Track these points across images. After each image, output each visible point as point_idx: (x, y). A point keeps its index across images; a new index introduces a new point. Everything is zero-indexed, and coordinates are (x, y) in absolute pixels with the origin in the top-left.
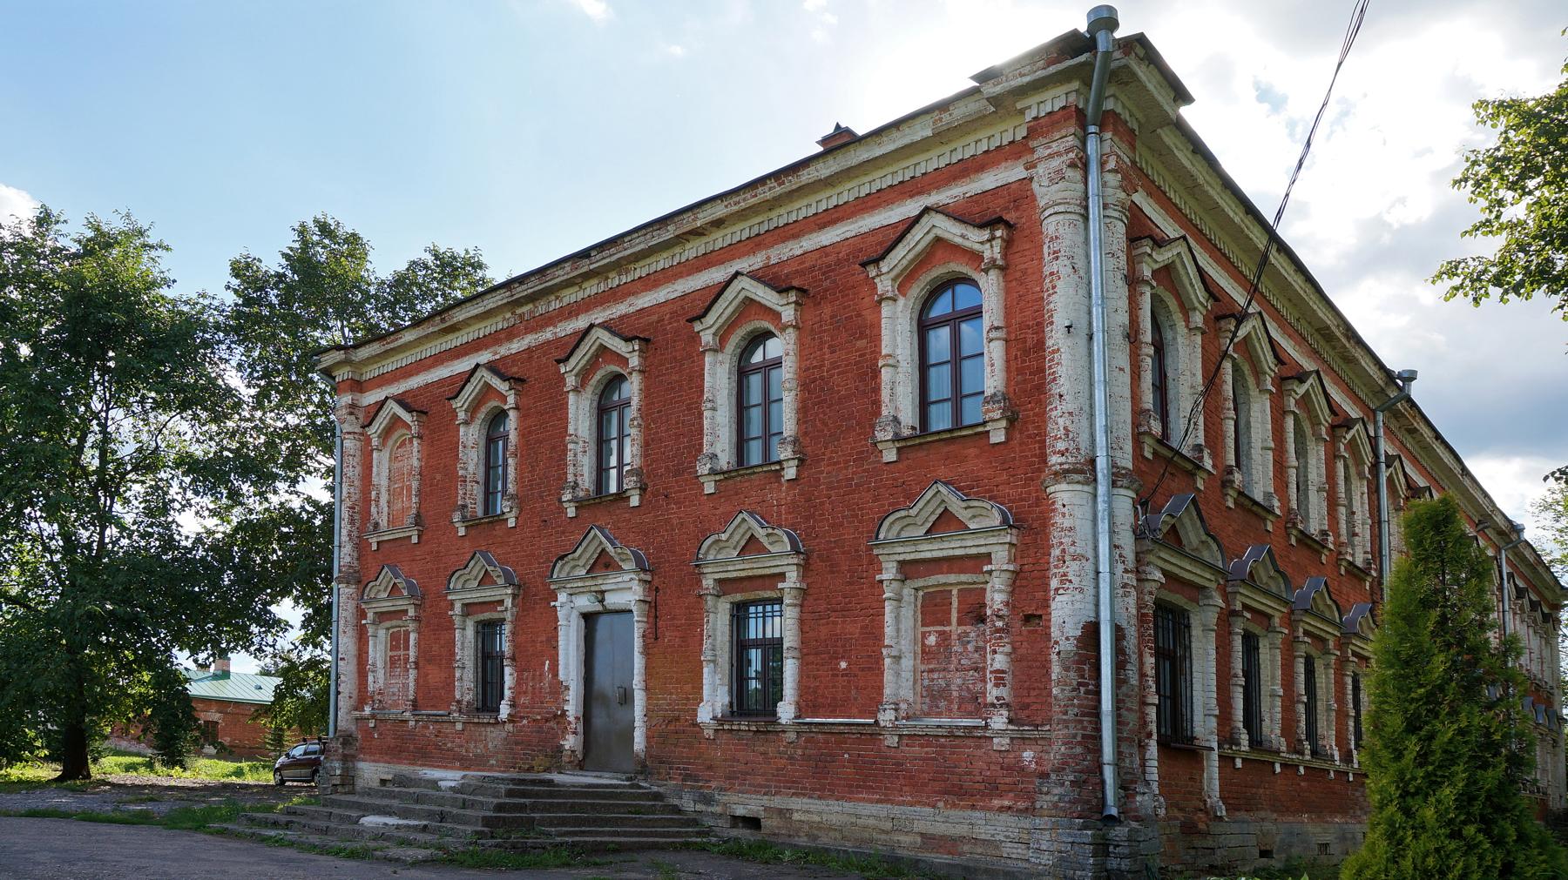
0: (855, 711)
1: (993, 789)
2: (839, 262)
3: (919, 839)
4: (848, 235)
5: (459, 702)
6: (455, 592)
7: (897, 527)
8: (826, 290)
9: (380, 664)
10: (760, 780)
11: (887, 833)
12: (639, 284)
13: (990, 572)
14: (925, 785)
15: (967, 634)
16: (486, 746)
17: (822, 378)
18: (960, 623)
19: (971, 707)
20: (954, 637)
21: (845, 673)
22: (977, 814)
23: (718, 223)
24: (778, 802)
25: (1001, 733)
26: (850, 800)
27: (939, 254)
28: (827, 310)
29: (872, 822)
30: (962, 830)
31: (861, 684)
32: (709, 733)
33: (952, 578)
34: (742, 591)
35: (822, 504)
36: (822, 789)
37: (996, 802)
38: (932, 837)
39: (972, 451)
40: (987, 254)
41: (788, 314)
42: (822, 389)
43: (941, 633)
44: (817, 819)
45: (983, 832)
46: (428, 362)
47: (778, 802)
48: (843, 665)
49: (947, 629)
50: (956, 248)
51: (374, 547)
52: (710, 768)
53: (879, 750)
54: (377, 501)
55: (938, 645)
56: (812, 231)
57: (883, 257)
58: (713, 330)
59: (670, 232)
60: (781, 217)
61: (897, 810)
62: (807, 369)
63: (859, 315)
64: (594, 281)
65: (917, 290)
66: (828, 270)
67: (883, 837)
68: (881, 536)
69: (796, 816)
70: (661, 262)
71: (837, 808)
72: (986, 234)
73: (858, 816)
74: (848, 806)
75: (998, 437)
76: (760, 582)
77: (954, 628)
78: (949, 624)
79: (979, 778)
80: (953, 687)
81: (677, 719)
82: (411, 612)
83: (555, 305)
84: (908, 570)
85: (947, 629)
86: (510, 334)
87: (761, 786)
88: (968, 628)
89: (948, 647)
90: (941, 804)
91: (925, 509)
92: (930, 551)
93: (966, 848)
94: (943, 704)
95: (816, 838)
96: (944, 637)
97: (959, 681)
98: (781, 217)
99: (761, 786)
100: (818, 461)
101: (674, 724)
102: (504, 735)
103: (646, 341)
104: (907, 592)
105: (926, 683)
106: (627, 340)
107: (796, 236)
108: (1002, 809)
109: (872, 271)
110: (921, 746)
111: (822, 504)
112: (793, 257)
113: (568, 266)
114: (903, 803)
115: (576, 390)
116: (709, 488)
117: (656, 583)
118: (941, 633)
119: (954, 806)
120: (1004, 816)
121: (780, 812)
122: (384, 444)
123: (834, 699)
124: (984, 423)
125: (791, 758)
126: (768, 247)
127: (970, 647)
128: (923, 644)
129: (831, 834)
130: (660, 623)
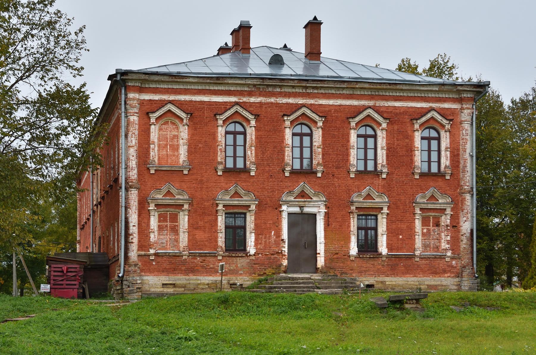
0: (405, 251)
1: (445, 271)
2: (400, 113)
8: (396, 121)
10: (372, 273)
15: (435, 229)
17: (394, 148)
18: (433, 226)
19: (436, 250)
21: (401, 239)
24: (380, 279)
25: (448, 257)
26: (405, 277)
28: (396, 127)
29: (412, 283)
30: (439, 283)
31: (407, 243)
33: (430, 214)
34: (364, 211)
36: (394, 274)
37: (446, 275)
38: (430, 286)
39: (440, 180)
41: (384, 125)
43: (428, 229)
45: (444, 283)
47: (380, 279)
48: (401, 237)
55: (427, 232)
56: (392, 100)
61: (420, 279)
62: (389, 144)
63: (406, 132)
66: (396, 114)
69: (387, 283)
75: (448, 177)
76: (371, 209)
77: (431, 228)
78: (430, 226)
81: (337, 254)
89: (430, 233)
94: (428, 249)
96: (429, 230)
100: (393, 174)
109: (415, 122)
112: (384, 106)
114: (420, 277)
119: (435, 277)
120: (450, 278)
121: (382, 282)
123: (398, 247)
125: (383, 265)
126: (376, 100)
127: (436, 233)
129: (399, 287)
130: (330, 220)
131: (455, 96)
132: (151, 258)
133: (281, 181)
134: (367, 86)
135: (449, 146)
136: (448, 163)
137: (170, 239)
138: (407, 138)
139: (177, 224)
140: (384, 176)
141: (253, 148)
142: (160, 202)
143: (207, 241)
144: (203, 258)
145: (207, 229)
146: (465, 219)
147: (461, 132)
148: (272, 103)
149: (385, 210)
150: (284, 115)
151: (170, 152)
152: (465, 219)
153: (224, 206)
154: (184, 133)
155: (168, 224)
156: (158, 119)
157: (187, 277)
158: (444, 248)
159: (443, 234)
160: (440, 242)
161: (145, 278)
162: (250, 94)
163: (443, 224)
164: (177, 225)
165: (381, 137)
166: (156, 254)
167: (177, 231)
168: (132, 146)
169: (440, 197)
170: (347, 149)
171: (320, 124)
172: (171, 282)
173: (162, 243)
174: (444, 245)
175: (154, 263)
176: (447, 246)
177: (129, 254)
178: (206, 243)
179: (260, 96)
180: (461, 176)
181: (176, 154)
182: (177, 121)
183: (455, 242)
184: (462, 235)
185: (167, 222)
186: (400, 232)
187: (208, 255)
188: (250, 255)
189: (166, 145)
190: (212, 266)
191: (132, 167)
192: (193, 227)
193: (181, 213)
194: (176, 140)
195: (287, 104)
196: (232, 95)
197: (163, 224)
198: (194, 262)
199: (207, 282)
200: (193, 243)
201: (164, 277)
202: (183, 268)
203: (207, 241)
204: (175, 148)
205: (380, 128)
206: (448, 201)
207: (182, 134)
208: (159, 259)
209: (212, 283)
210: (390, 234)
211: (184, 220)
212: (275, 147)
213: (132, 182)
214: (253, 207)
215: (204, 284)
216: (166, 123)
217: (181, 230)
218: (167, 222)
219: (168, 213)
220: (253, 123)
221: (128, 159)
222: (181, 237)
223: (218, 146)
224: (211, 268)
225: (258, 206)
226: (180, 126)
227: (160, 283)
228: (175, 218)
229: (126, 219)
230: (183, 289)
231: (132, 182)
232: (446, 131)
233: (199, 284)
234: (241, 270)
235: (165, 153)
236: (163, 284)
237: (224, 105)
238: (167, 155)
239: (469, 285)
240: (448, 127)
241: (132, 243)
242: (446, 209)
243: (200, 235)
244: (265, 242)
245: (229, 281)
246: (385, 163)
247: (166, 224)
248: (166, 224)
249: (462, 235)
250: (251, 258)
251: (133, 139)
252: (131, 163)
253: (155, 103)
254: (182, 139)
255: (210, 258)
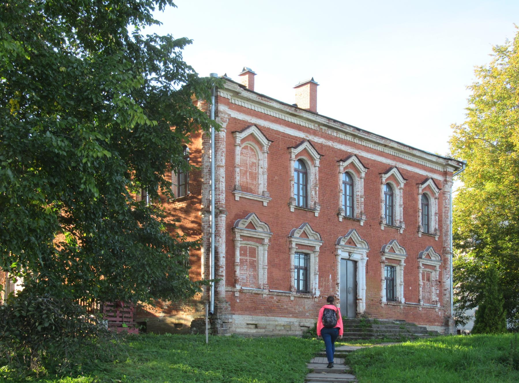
1: (435, 321)
16: (304, 308)
23: (392, 148)
41: (402, 185)
59: (382, 142)
60: (401, 155)
64: (351, 137)
70: (371, 145)
76: (395, 261)
98: (401, 155)
101: (373, 302)
102: (313, 303)
107: (403, 163)
108: (438, 325)
113: (352, 129)
131: (440, 169)
132: (236, 295)
133: (336, 226)
134: (395, 146)
135: (437, 212)
136: (437, 227)
137: (250, 275)
138: (414, 200)
139: (255, 259)
140: (402, 232)
141: (317, 188)
142: (246, 233)
143: (282, 280)
144: (279, 298)
145: (282, 267)
146: (448, 276)
147: (444, 201)
148: (329, 146)
149: (403, 263)
150: (341, 160)
151: (249, 181)
152: (448, 276)
153: (297, 244)
154: (264, 161)
155: (248, 258)
156: (243, 140)
157: (267, 318)
158: (435, 300)
159: (433, 288)
160: (430, 295)
161: (234, 316)
162: (315, 133)
163: (433, 279)
164: (255, 261)
165: (399, 196)
166: (241, 291)
167: (255, 267)
168: (222, 166)
169: (433, 255)
170: (379, 203)
171: (363, 175)
172: (253, 322)
173: (243, 279)
174: (435, 298)
175: (238, 301)
176: (437, 299)
177: (219, 289)
178: (281, 282)
179: (322, 137)
180: (444, 239)
181: (254, 183)
182: (257, 147)
183: (441, 295)
184: (445, 290)
185: (247, 256)
186: (411, 284)
187: (284, 294)
188: (316, 297)
189: (246, 171)
190: (285, 307)
191: (222, 191)
192: (271, 263)
193: (261, 248)
194: (254, 168)
195: (340, 150)
196: (301, 131)
197: (243, 258)
198: (271, 302)
199: (283, 323)
200: (272, 283)
201: (248, 316)
202: (263, 307)
203: (282, 280)
204: (254, 177)
205: (399, 187)
206: (437, 259)
207: (261, 162)
208: (243, 297)
209: (287, 325)
211: (263, 255)
212: (332, 191)
213: (222, 207)
214: (318, 249)
215: (280, 326)
216: (246, 148)
217: (261, 266)
218: (247, 256)
219: (248, 246)
220: (317, 162)
221: (217, 180)
222: (259, 274)
223: (291, 180)
224: (285, 309)
225: (321, 247)
226: (260, 153)
227: (244, 323)
228: (253, 253)
229: (216, 248)
230: (264, 330)
231: (222, 207)
232: (436, 198)
233: (276, 325)
234: (307, 312)
235: (245, 180)
236: (247, 324)
237: (294, 139)
238: (247, 182)
240: (437, 195)
241: (223, 276)
243: (278, 274)
244: (325, 285)
245: (300, 323)
246: (402, 220)
247: (246, 258)
248: (246, 258)
249: (445, 290)
250: (316, 300)
251: (223, 158)
252: (221, 185)
253: (239, 123)
254: (262, 168)
255: (284, 297)
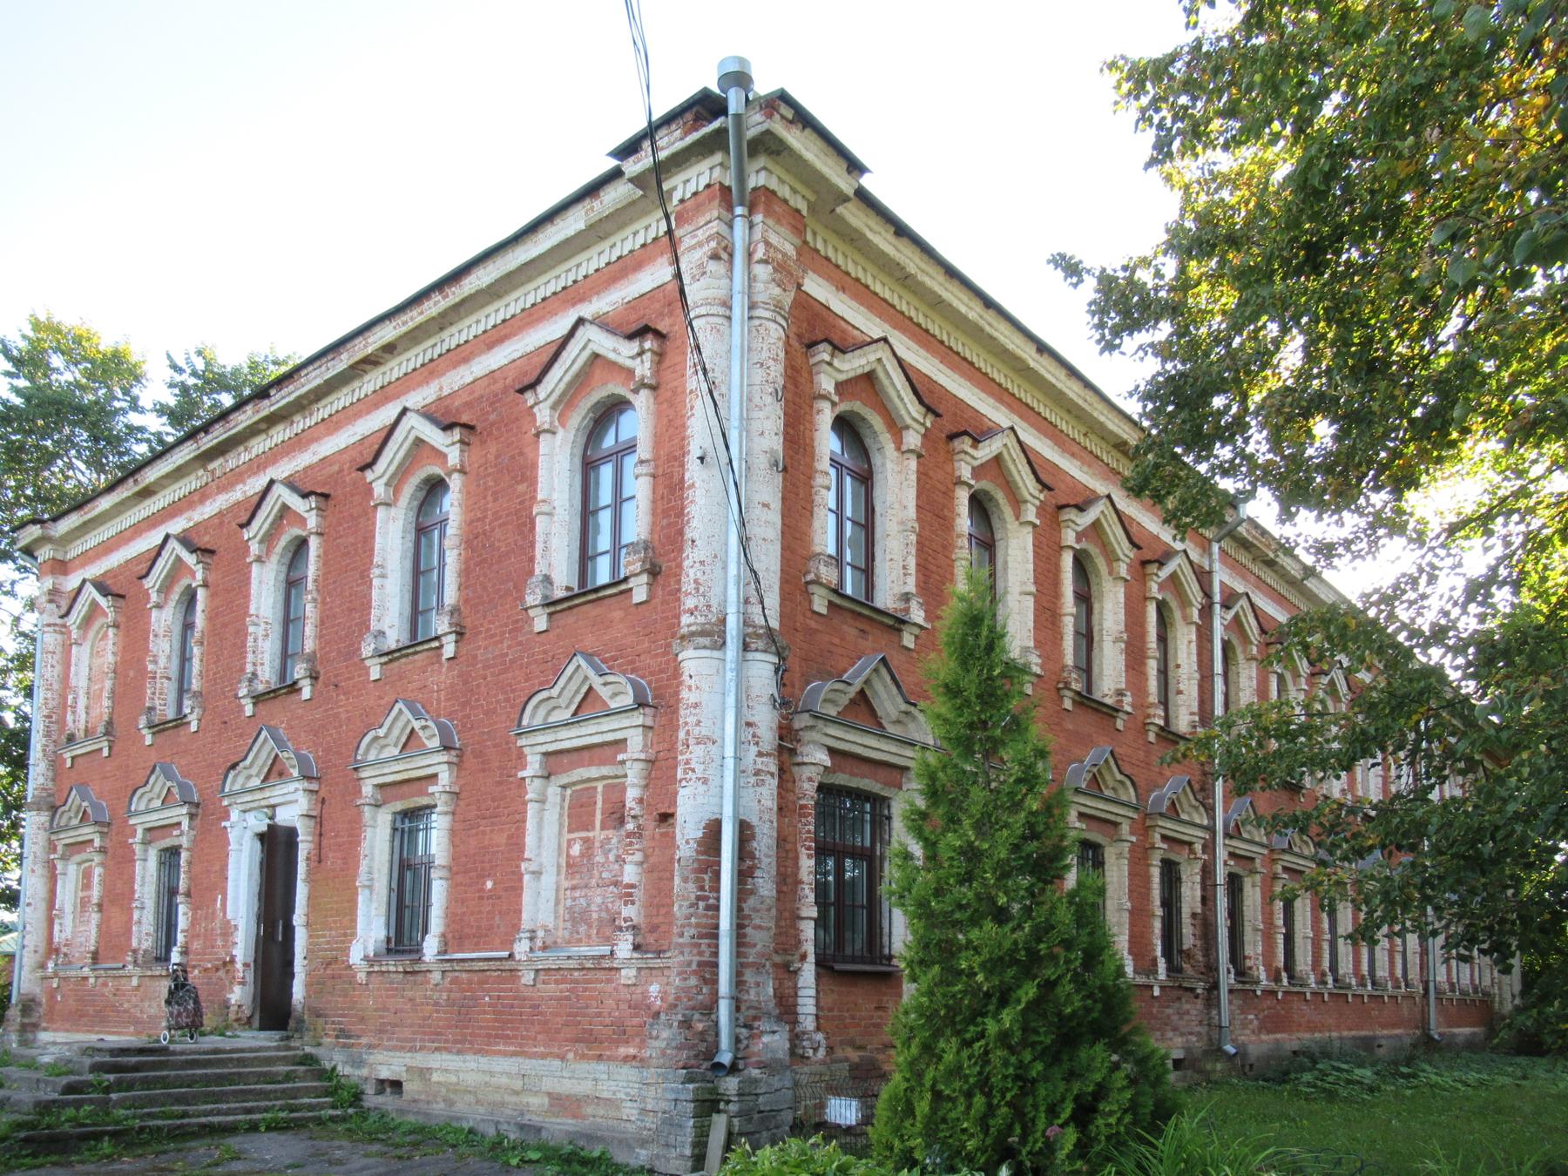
3: (546, 1100)
4: (516, 355)
5: (135, 951)
6: (138, 814)
7: (542, 712)
8: (492, 425)
9: (68, 908)
10: (407, 1033)
11: (517, 1093)
12: (322, 427)
13: (623, 762)
14: (558, 1031)
15: (608, 839)
18: (603, 828)
20: (597, 844)
22: (602, 1067)
23: (390, 349)
24: (419, 1060)
27: (598, 373)
29: (504, 1080)
30: (584, 1088)
32: (361, 977)
33: (594, 772)
34: (402, 798)
35: (478, 686)
37: (623, 1051)
39: (617, 614)
40: (638, 373)
42: (484, 546)
43: (586, 840)
44: (454, 1079)
46: (127, 534)
49: (591, 834)
50: (613, 365)
51: (69, 764)
52: (362, 1020)
53: (518, 991)
54: (74, 707)
55: (582, 855)
56: (481, 352)
57: (538, 381)
58: (384, 479)
61: (528, 1065)
62: (472, 521)
63: (521, 454)
64: (280, 427)
65: (579, 417)
66: (494, 400)
67: (514, 1099)
68: (525, 722)
69: (435, 1077)
71: (473, 1065)
72: (634, 347)
73: (492, 1074)
74: (484, 1062)
79: (608, 1020)
80: (594, 908)
82: (97, 843)
83: (244, 457)
84: (555, 761)
85: (591, 834)
86: (202, 495)
87: (406, 1040)
88: (610, 833)
90: (571, 1056)
91: (566, 691)
92: (571, 738)
93: (589, 1110)
95: (450, 1103)
97: (599, 900)
99: (406, 1040)
103: (326, 496)
104: (553, 791)
105: (569, 903)
106: (305, 496)
107: (466, 360)
108: (626, 1059)
110: (557, 982)
111: (478, 686)
115: (259, 560)
116: (375, 673)
117: (322, 794)
118: (586, 840)
119: (583, 1057)
122: (84, 637)
123: (479, 927)
124: (626, 579)
127: (612, 858)
128: (568, 855)
130: (324, 842)
210: (460, 878)
239: (663, 1105)
242: (625, 740)
